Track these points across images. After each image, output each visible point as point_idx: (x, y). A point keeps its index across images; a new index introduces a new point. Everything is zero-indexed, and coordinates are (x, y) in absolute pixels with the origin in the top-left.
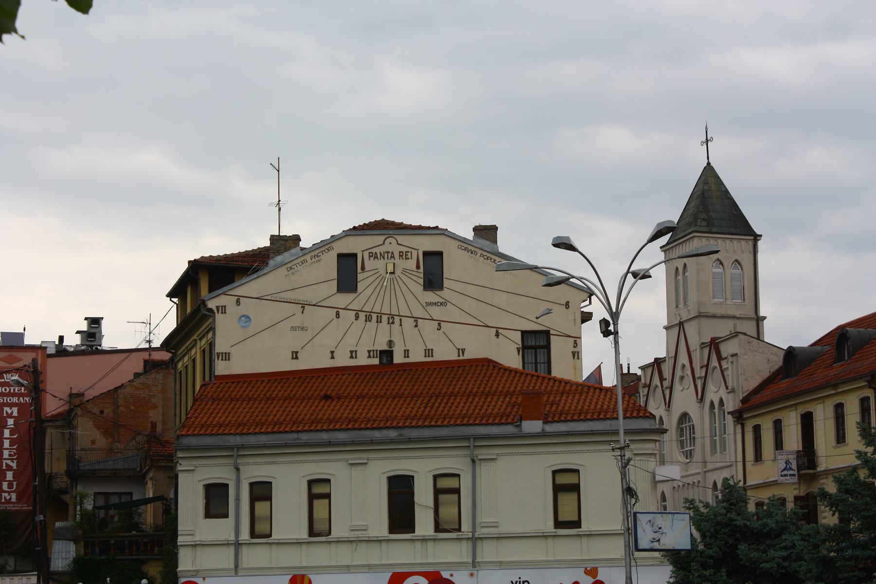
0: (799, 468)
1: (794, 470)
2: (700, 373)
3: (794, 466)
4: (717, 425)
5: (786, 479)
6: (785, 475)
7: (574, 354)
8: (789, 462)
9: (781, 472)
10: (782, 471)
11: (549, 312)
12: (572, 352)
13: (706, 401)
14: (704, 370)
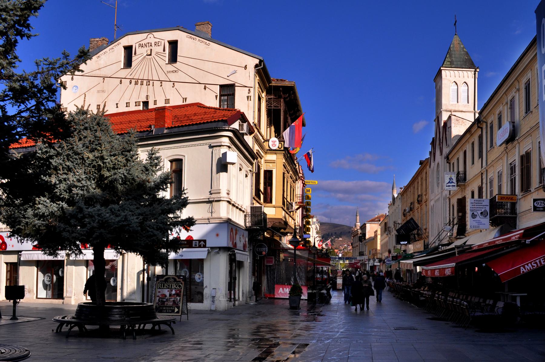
3: (455, 181)
5: (449, 188)
6: (449, 186)
7: (248, 97)
9: (447, 184)
10: (447, 184)
11: (235, 72)
12: (247, 96)
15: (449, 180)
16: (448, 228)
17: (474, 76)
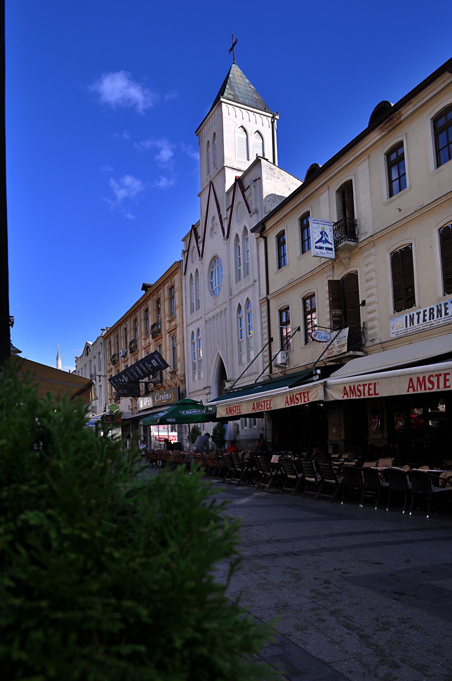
0: (337, 243)
1: (332, 244)
2: (225, 214)
3: (331, 239)
4: (241, 256)
6: (321, 248)
8: (325, 233)
9: (316, 243)
10: (316, 243)
13: (231, 238)
15: (320, 236)
17: (271, 125)
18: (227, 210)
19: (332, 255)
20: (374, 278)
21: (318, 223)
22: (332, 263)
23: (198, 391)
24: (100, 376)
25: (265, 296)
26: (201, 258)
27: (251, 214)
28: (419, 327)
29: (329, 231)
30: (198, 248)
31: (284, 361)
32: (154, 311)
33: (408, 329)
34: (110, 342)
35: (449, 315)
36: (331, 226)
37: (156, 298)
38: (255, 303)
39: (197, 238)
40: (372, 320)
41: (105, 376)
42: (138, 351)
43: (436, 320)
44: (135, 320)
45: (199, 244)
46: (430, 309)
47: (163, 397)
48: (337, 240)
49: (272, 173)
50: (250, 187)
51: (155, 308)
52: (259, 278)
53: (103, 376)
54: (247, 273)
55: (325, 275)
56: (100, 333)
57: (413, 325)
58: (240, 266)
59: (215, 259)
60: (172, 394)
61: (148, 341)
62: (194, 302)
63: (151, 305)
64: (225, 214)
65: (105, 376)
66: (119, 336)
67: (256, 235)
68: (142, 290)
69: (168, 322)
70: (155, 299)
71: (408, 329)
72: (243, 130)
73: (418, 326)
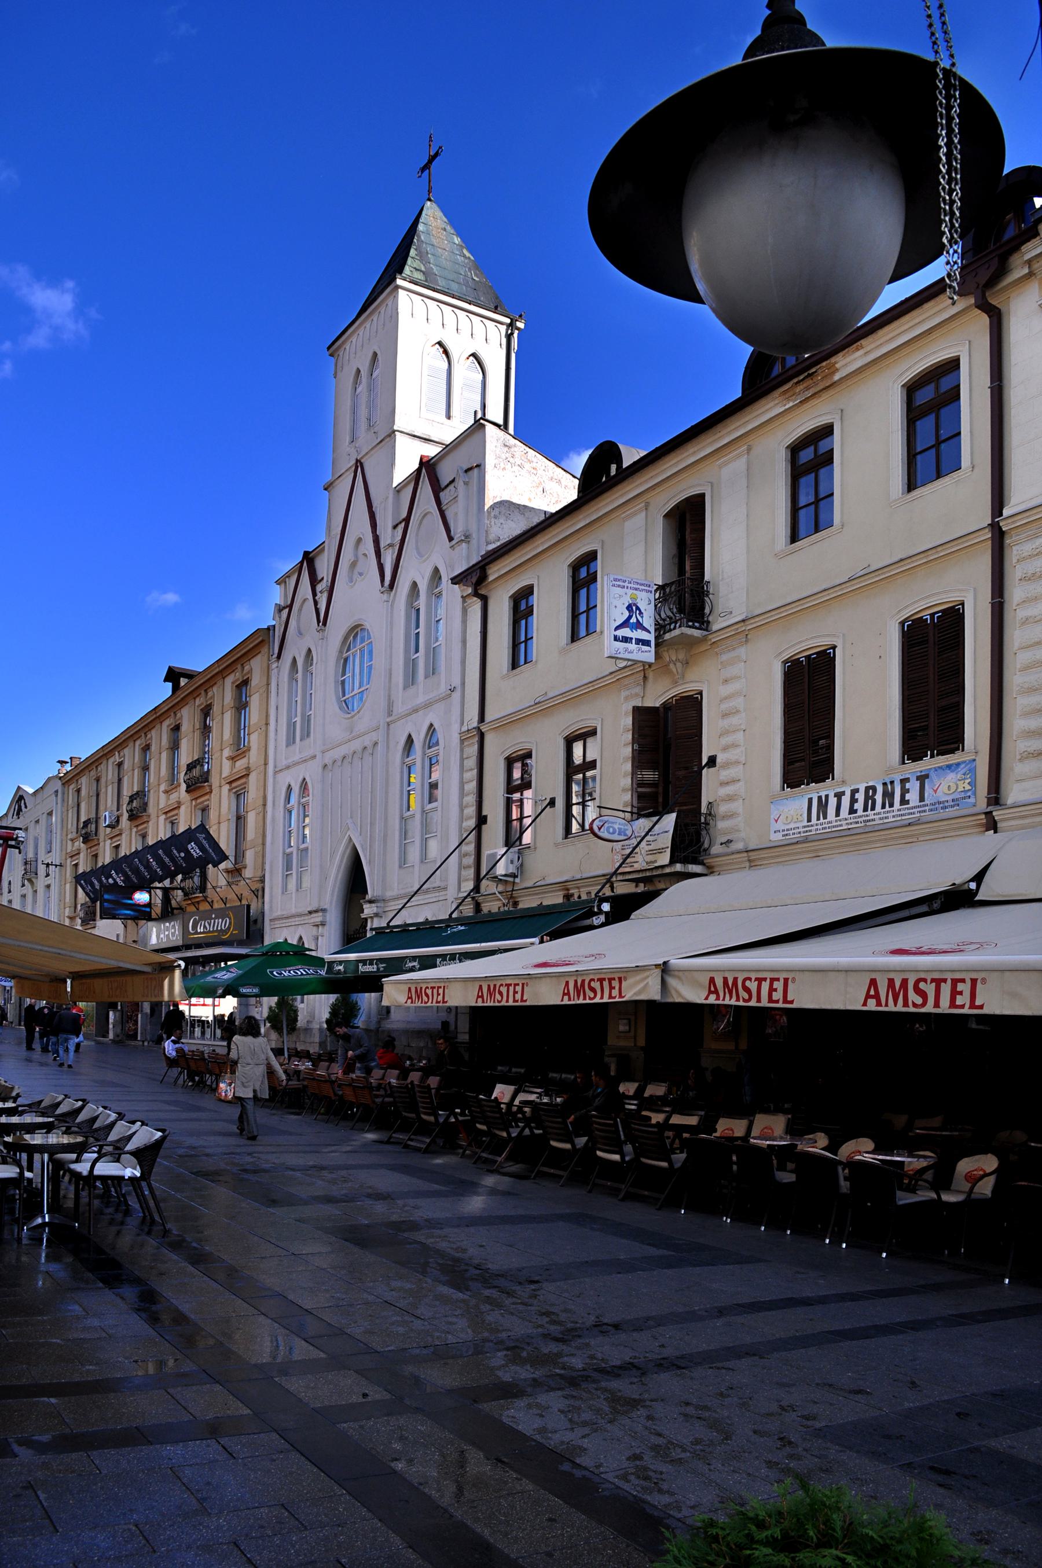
0: (661, 628)
1: (649, 632)
2: (388, 536)
3: (648, 621)
4: (422, 630)
6: (626, 640)
8: (638, 608)
13: (399, 590)
14: (400, 529)
15: (627, 614)
16: (616, 826)
17: (504, 341)
18: (395, 527)
19: (648, 655)
20: (742, 710)
21: (624, 587)
22: (644, 670)
23: (293, 916)
24: (48, 865)
25: (475, 724)
26: (323, 628)
27: (454, 542)
28: (839, 823)
29: (646, 603)
30: (316, 603)
31: (512, 869)
32: (194, 732)
33: (812, 826)
34: (79, 791)
35: (911, 804)
36: (651, 592)
37: (202, 704)
38: (450, 738)
39: (314, 581)
40: (730, 798)
41: (61, 865)
42: (149, 816)
43: (879, 814)
44: (146, 748)
45: (319, 595)
46: (867, 789)
47: (210, 925)
48: (661, 622)
49: (507, 455)
50: (455, 484)
51: (197, 726)
52: (463, 684)
53: (56, 866)
54: (432, 670)
55: (624, 694)
56: (54, 770)
57: (825, 817)
58: (417, 651)
59: (356, 631)
60: (230, 919)
61: (174, 797)
62: (298, 719)
63: (188, 717)
64: (388, 536)
65: (61, 865)
66: (103, 780)
67: (462, 591)
68: (166, 680)
69: (228, 759)
70: (198, 706)
71: (812, 826)
72: (441, 350)
73: (836, 821)
